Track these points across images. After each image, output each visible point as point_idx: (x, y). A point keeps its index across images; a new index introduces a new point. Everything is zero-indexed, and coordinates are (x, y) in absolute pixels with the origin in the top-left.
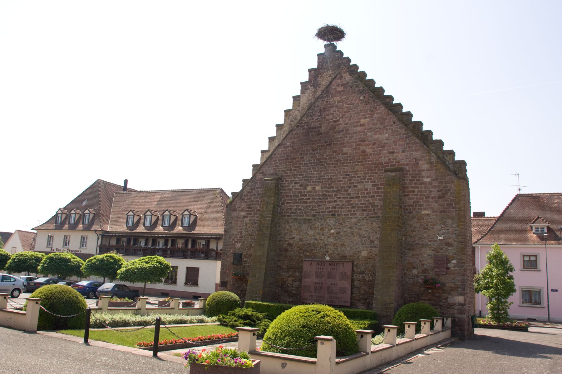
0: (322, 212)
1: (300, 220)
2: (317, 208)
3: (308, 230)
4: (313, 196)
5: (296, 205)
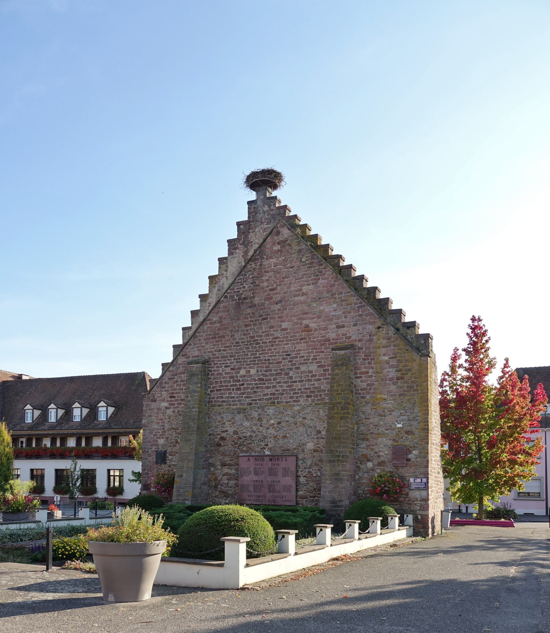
0: (259, 400)
1: (233, 409)
2: (253, 396)
3: (243, 421)
4: (248, 381)
5: (228, 392)
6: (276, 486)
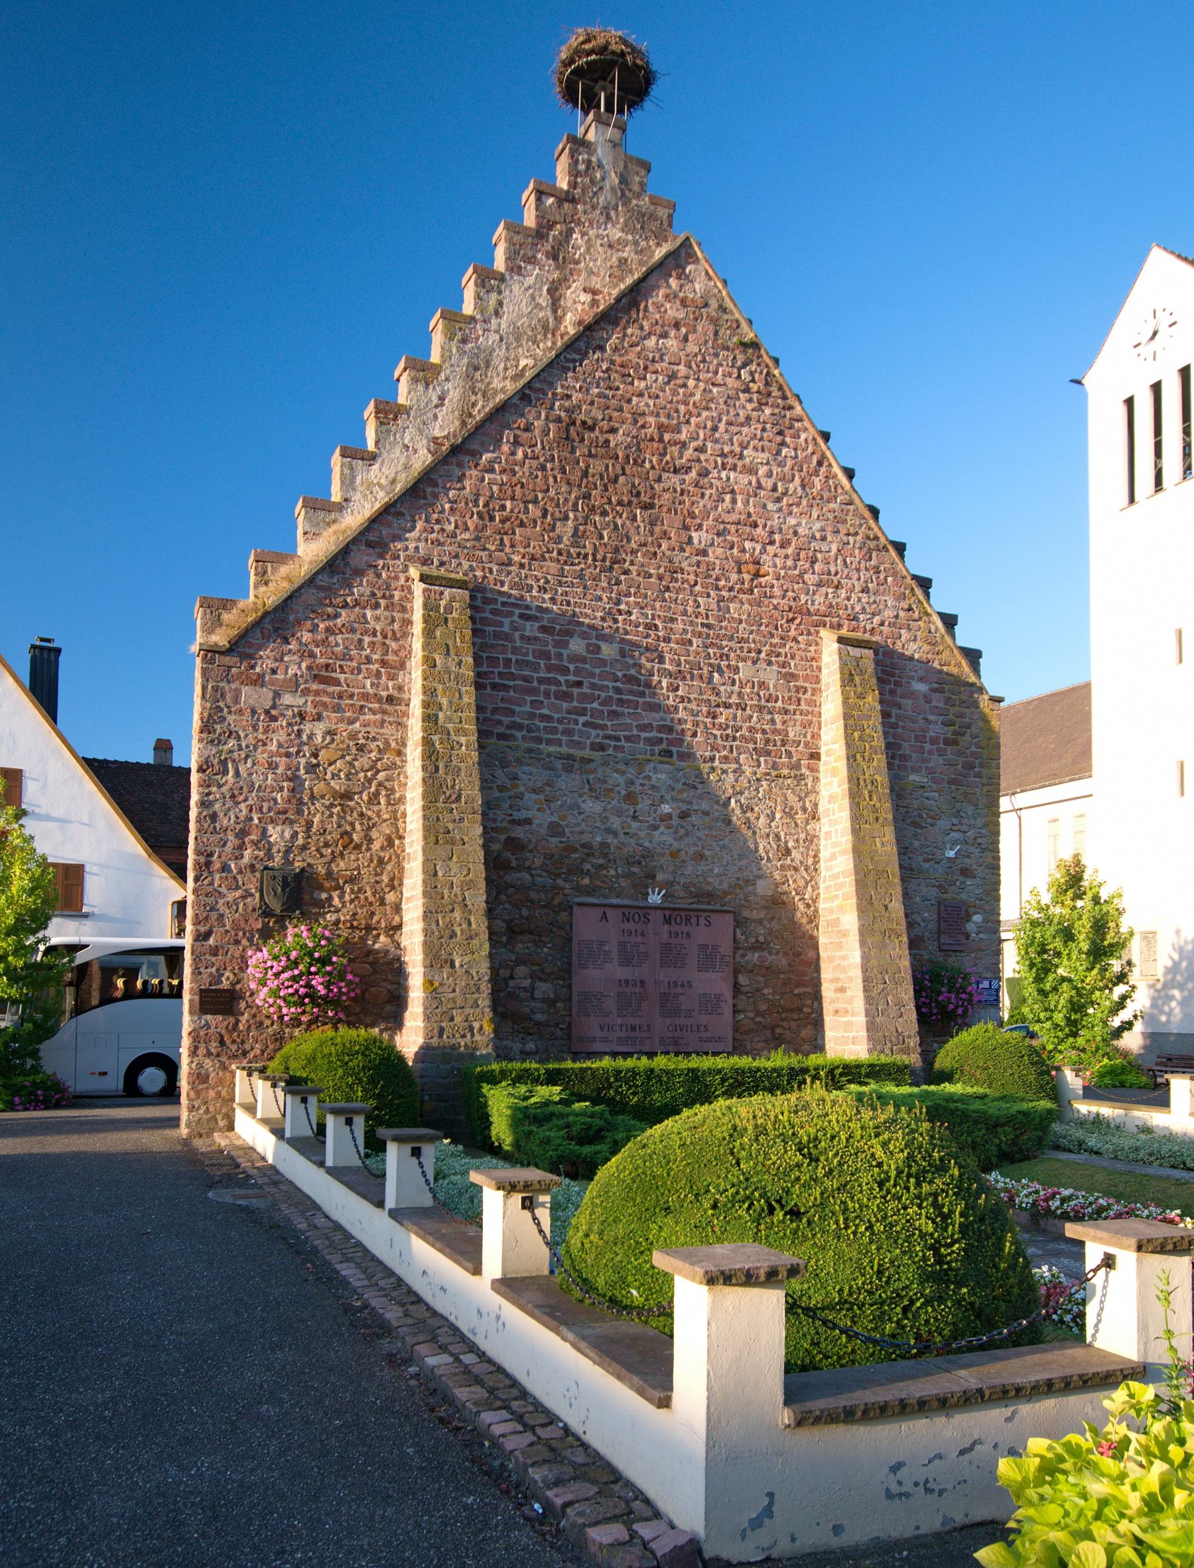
0: (627, 739)
1: (549, 755)
2: (609, 723)
3: (581, 796)
4: (593, 675)
5: (529, 699)
6: (681, 998)
